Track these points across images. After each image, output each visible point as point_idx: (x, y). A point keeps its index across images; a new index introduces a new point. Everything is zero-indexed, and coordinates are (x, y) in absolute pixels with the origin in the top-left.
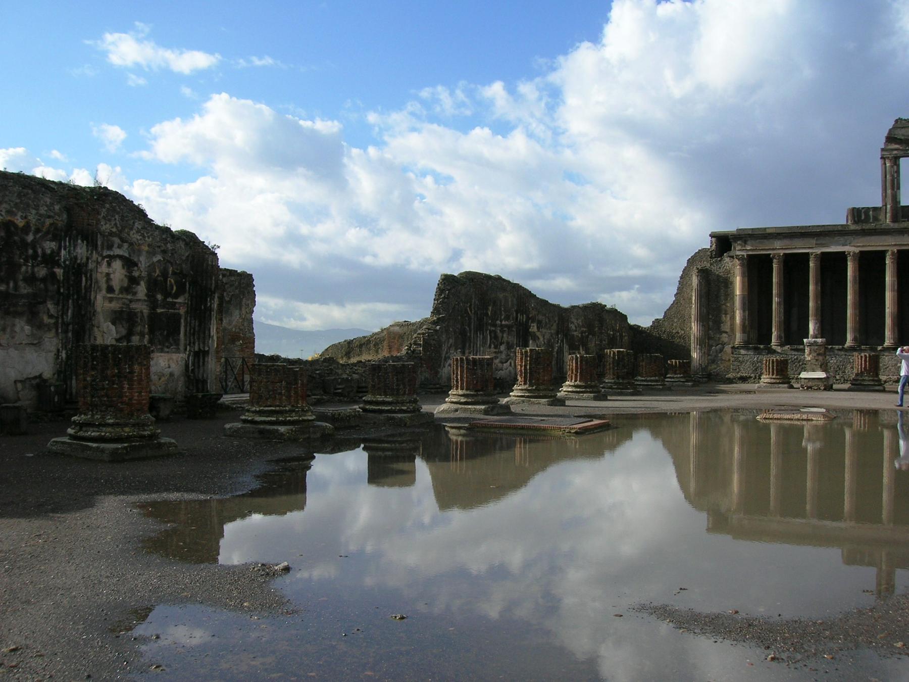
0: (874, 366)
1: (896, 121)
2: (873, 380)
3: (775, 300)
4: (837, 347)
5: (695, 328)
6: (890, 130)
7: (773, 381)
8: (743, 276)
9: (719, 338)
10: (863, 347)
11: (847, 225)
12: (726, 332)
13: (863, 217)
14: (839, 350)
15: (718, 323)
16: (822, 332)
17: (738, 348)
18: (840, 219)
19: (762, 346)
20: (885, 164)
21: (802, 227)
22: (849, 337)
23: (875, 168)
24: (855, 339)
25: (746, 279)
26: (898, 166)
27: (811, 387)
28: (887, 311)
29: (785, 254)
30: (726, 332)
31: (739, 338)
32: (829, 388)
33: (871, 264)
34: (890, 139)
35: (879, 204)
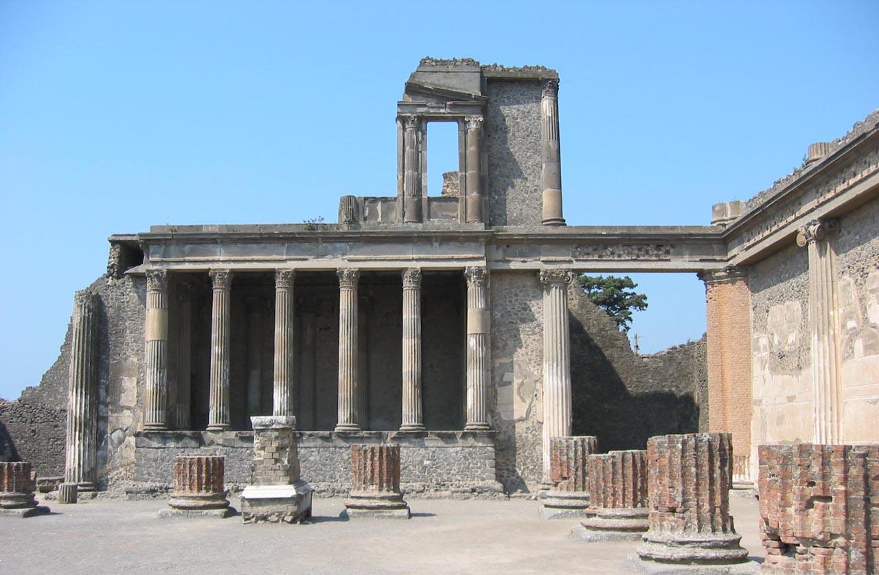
0: (391, 471)
1: (423, 63)
2: (391, 499)
3: (216, 350)
4: (321, 433)
5: (75, 403)
6: (413, 76)
7: (191, 503)
8: (160, 306)
9: (117, 418)
10: (364, 433)
11: (338, 226)
12: (129, 408)
13: (367, 214)
14: (323, 438)
15: (114, 389)
16: (296, 404)
17: (146, 435)
18: (330, 215)
19: (188, 433)
20: (404, 129)
21: (265, 227)
22: (343, 415)
23: (391, 134)
24: (353, 418)
25: (166, 314)
26: (424, 133)
27: (264, 518)
28: (404, 370)
29: (233, 271)
30: (129, 408)
31: (150, 417)
32: (304, 516)
33: (379, 291)
34: (413, 89)
35: (392, 191)
